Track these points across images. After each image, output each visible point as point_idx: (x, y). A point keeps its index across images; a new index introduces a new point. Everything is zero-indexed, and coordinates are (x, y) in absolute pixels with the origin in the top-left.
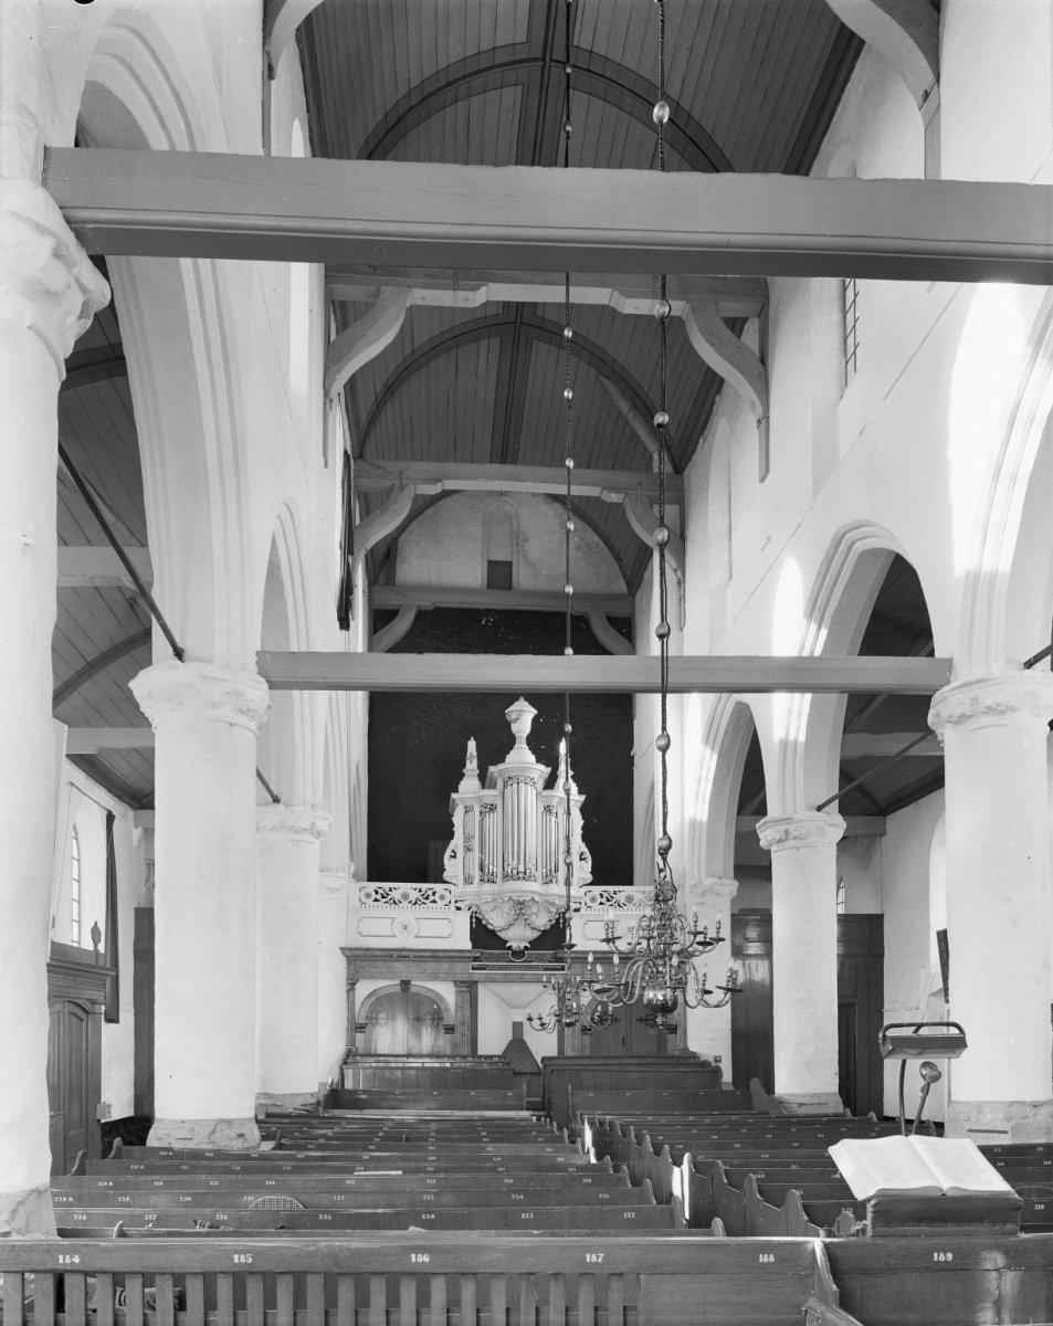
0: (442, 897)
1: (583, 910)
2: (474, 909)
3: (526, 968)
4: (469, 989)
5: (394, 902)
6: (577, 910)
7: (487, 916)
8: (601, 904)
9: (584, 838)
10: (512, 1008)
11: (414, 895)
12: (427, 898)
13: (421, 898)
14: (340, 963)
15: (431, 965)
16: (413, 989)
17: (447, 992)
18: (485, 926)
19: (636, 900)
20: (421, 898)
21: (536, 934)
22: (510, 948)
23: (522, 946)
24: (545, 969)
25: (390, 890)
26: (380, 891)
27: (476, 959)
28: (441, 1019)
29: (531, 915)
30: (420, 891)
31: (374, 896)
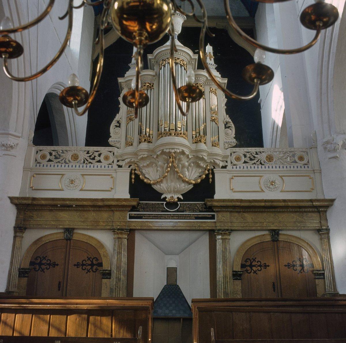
0: (107, 158)
1: (230, 167)
3: (179, 217)
6: (224, 167)
7: (144, 171)
8: (245, 162)
9: (228, 112)
12: (94, 159)
13: (88, 158)
14: (10, 215)
15: (92, 215)
17: (106, 239)
18: (142, 181)
20: (88, 158)
23: (175, 197)
24: (197, 218)
25: (63, 152)
26: (54, 153)
27: (134, 208)
28: (100, 265)
31: (48, 157)
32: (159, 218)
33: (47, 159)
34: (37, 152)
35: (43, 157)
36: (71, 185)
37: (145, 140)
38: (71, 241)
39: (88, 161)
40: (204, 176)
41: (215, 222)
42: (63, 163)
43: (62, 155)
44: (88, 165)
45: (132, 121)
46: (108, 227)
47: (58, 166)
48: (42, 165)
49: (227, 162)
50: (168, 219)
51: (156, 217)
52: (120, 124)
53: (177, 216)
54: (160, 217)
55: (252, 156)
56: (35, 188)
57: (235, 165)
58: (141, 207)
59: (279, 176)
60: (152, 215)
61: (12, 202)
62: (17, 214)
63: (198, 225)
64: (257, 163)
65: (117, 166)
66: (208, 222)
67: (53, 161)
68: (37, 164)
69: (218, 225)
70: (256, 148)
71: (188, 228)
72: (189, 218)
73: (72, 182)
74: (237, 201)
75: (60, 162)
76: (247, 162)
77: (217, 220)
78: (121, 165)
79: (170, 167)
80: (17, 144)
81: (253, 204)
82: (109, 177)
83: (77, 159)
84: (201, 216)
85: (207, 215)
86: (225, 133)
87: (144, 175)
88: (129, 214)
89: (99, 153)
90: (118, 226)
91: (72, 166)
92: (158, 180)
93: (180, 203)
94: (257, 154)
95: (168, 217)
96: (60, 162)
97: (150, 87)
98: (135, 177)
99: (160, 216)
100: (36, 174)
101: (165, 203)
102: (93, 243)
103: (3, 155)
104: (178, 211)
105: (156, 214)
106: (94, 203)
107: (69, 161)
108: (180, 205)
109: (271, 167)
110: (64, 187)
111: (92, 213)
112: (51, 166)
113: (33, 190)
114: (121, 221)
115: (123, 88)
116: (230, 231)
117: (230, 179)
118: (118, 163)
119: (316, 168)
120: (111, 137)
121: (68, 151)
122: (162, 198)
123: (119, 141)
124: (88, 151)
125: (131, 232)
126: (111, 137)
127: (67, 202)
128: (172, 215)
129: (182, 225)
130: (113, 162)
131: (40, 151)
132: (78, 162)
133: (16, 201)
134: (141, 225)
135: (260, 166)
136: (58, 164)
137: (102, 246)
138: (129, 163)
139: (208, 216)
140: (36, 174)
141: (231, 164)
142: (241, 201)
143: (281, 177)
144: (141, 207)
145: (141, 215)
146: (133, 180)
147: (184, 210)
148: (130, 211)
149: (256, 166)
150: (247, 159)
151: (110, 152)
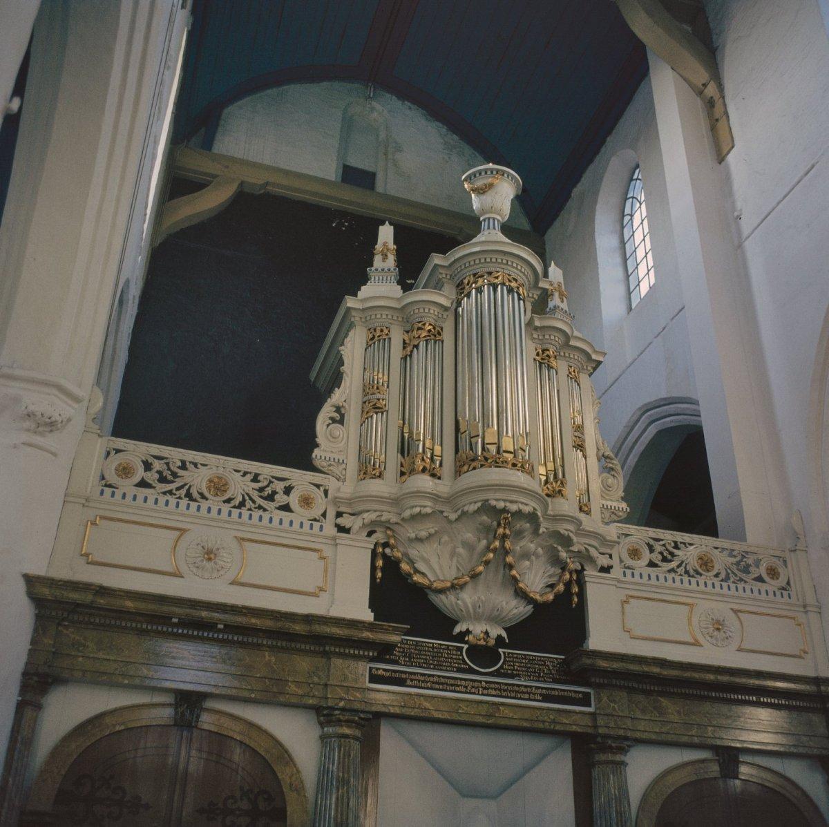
0: (306, 502)
1: (616, 572)
2: (379, 536)
3: (503, 691)
4: (357, 734)
5: (189, 495)
6: (606, 569)
8: (652, 564)
10: (464, 796)
11: (239, 486)
12: (271, 498)
13: (255, 495)
16: (207, 721)
17: (296, 735)
18: (404, 578)
19: (718, 567)
20: (255, 495)
21: (517, 610)
22: (461, 637)
24: (546, 698)
25: (183, 466)
26: (157, 465)
27: (384, 652)
29: (526, 555)
30: (255, 479)
31: (140, 473)
32: (451, 688)
33: (137, 479)
34: (108, 453)
35: (125, 471)
36: (208, 565)
37: (424, 470)
38: (195, 734)
39: (254, 502)
40: (561, 587)
41: (593, 715)
42: (183, 496)
43: (181, 472)
44: (256, 514)
45: (380, 414)
46: (311, 702)
47: (167, 503)
48: (119, 494)
49: (611, 556)
50: (474, 693)
51: (442, 684)
52: (342, 416)
53: (497, 686)
54: (452, 685)
55: (667, 550)
56: (95, 559)
57: (628, 568)
58: (403, 652)
59: (732, 609)
60: (431, 679)
61: (31, 595)
62: (36, 630)
63: (551, 717)
64: (679, 570)
65: (336, 529)
66: (574, 712)
67: (154, 488)
68: (106, 489)
69: (600, 722)
70: (675, 532)
71: (525, 724)
72: (527, 696)
73: (210, 555)
74: (654, 663)
75: (175, 494)
76: (655, 565)
77: (597, 708)
78: (347, 527)
79: (494, 551)
80: (69, 420)
81: (688, 674)
82: (315, 555)
83: (225, 491)
84: (556, 693)
85: (570, 691)
86: (603, 486)
87: (411, 562)
88: (371, 669)
89: (287, 484)
90: (341, 699)
91: (209, 510)
92: (455, 582)
93: (504, 653)
94: (676, 547)
95: (473, 687)
96: (175, 494)
97: (435, 336)
98: (384, 564)
99: (451, 682)
100: (102, 518)
101: (466, 646)
102: (261, 746)
103: (23, 444)
104: (497, 674)
105: (444, 677)
106: (280, 624)
107: (203, 497)
108: (505, 657)
109: (709, 583)
110: (184, 569)
111: (267, 654)
112: (146, 500)
113: (88, 563)
114: (349, 685)
115: (352, 326)
116: (625, 743)
117: (622, 605)
118: (340, 521)
119: (811, 600)
120: (317, 445)
121: (199, 466)
122: (454, 634)
123: (341, 461)
124: (257, 475)
125: (369, 724)
126: (317, 445)
127: (204, 614)
128: (483, 683)
129: (511, 715)
130: (324, 515)
131: (118, 451)
132: (224, 502)
133: (46, 592)
134: (402, 704)
135: (686, 578)
136: (168, 497)
137: (285, 756)
138: (373, 523)
139: (574, 695)
140: (102, 518)
141: (620, 564)
142: (662, 663)
143: (735, 612)
144: (403, 652)
145: (404, 676)
146: (379, 575)
147: (515, 672)
148: (373, 660)
149: (678, 579)
150: (656, 558)
151: (318, 486)
